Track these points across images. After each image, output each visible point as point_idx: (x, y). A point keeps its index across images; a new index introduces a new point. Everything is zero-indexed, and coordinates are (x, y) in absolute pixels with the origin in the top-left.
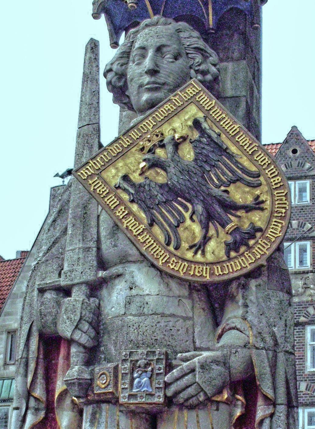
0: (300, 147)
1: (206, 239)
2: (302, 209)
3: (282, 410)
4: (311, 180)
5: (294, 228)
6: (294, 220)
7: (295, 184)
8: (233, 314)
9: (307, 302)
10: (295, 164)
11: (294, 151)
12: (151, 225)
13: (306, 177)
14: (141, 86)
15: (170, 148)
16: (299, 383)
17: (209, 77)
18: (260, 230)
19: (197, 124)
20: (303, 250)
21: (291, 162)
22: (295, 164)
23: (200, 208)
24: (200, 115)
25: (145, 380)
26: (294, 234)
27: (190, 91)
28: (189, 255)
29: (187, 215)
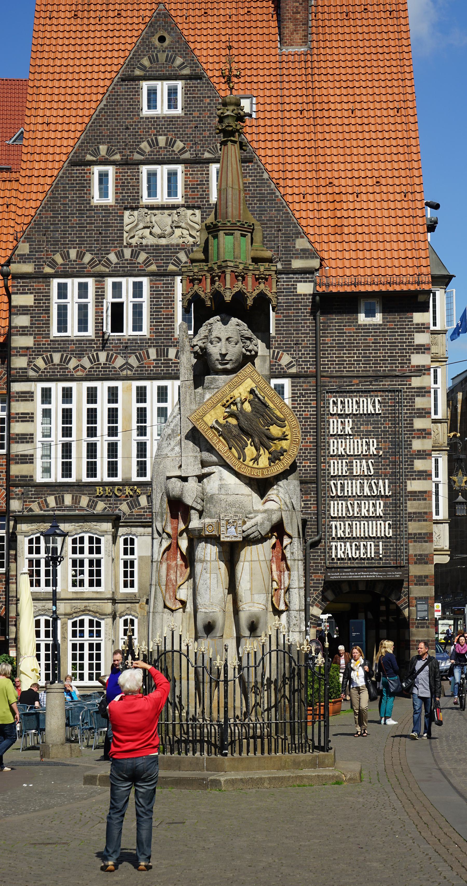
0: (169, 33)
1: (259, 455)
2: (172, 121)
3: (296, 540)
4: (184, 81)
5: (160, 145)
6: (161, 135)
7: (162, 85)
8: (272, 493)
9: (178, 245)
10: (162, 57)
11: (162, 39)
12: (230, 448)
13: (177, 78)
14: (218, 360)
15: (239, 405)
16: (168, 350)
17: (253, 353)
18: (286, 451)
19: (252, 392)
20: (172, 176)
21: (157, 55)
22: (162, 57)
23: (256, 440)
24: (253, 385)
25: (233, 529)
26: (161, 155)
27: (247, 370)
28: (251, 464)
29: (249, 442)
